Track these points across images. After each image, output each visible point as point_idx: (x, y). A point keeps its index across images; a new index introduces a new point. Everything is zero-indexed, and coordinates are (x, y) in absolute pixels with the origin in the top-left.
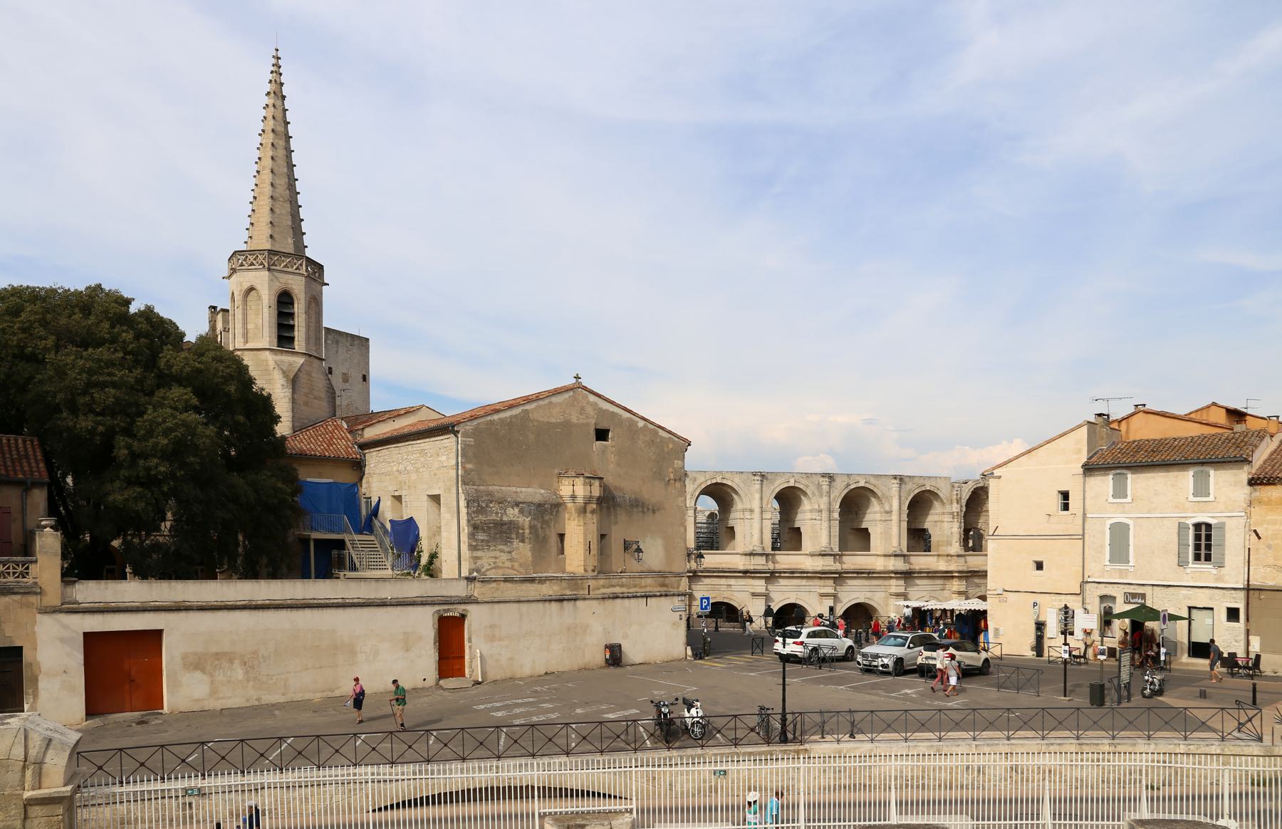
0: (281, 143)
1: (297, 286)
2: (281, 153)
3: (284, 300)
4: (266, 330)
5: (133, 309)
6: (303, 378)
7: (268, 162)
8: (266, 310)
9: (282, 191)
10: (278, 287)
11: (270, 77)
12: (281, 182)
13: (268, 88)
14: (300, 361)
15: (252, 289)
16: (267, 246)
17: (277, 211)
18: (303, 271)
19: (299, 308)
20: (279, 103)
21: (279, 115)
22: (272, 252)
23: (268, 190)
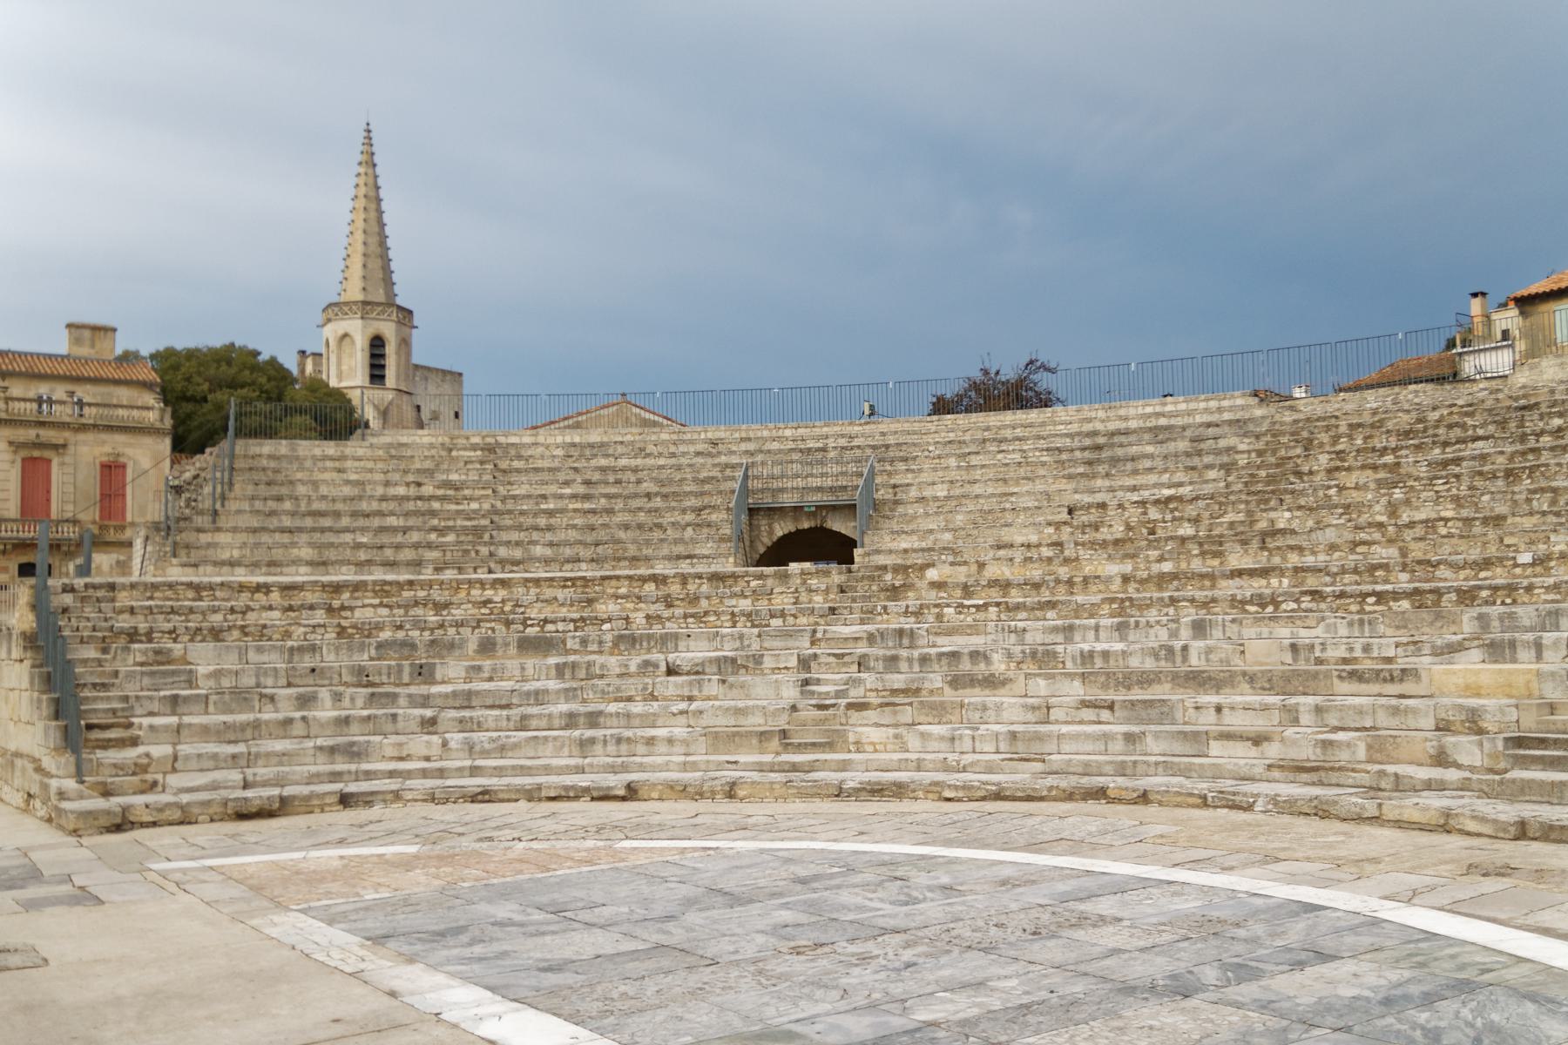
0: (373, 206)
1: (388, 330)
2: (373, 215)
3: (377, 343)
4: (359, 373)
5: (261, 358)
6: (394, 411)
7: (360, 224)
8: (359, 355)
9: (374, 247)
10: (371, 331)
11: (362, 148)
12: (373, 240)
13: (360, 158)
14: (390, 396)
15: (346, 335)
16: (360, 297)
17: (370, 266)
18: (394, 317)
19: (390, 349)
20: (370, 171)
21: (371, 181)
22: (365, 303)
23: (360, 248)
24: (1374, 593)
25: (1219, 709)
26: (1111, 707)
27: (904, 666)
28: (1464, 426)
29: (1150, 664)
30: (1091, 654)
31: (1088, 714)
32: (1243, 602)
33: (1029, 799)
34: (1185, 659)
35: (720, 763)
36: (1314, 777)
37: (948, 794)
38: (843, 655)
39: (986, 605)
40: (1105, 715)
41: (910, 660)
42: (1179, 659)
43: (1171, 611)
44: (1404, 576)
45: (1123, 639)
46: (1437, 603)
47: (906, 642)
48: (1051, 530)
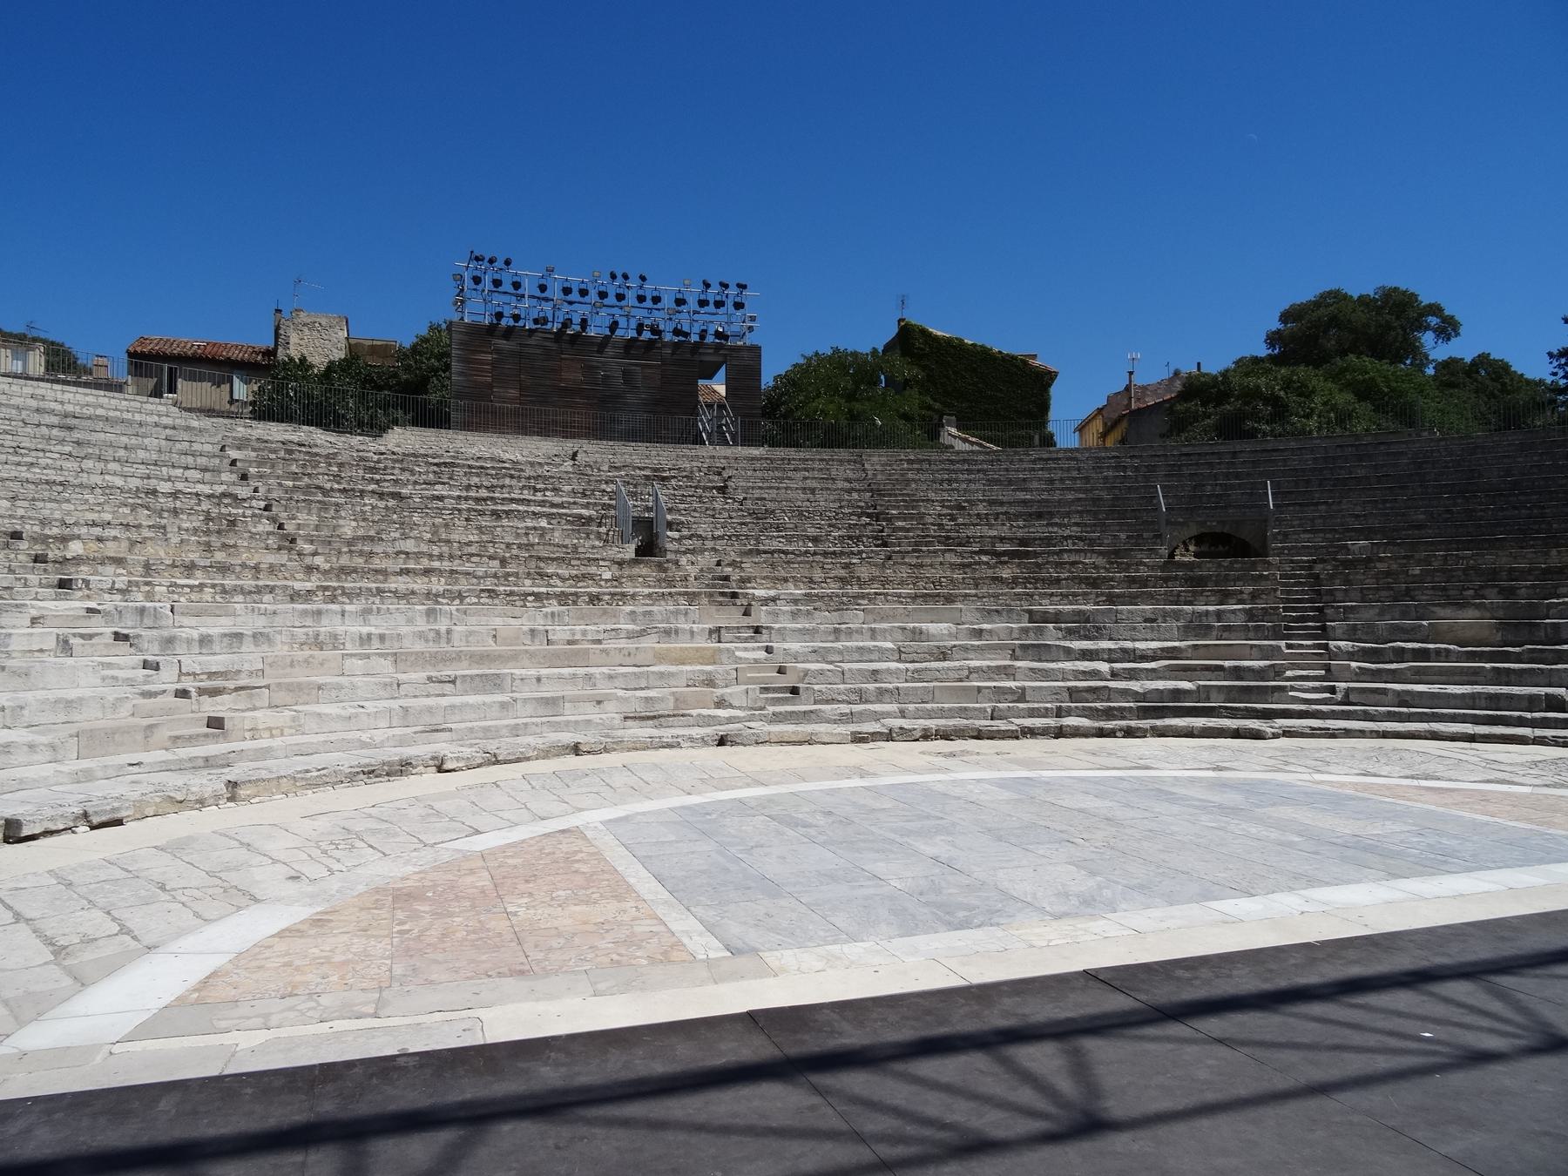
24: (532, 594)
25: (539, 680)
26: (453, 682)
27: (180, 648)
28: (412, 472)
29: (419, 647)
30: (369, 636)
31: (437, 688)
32: (437, 595)
33: (518, 760)
34: (449, 641)
35: (121, 767)
36: (656, 722)
37: (447, 766)
38: (91, 636)
39: (202, 586)
40: (448, 688)
41: (189, 641)
42: (443, 640)
43: (377, 600)
44: (528, 582)
45: (366, 623)
46: (575, 603)
47: (148, 622)
48: (127, 511)
